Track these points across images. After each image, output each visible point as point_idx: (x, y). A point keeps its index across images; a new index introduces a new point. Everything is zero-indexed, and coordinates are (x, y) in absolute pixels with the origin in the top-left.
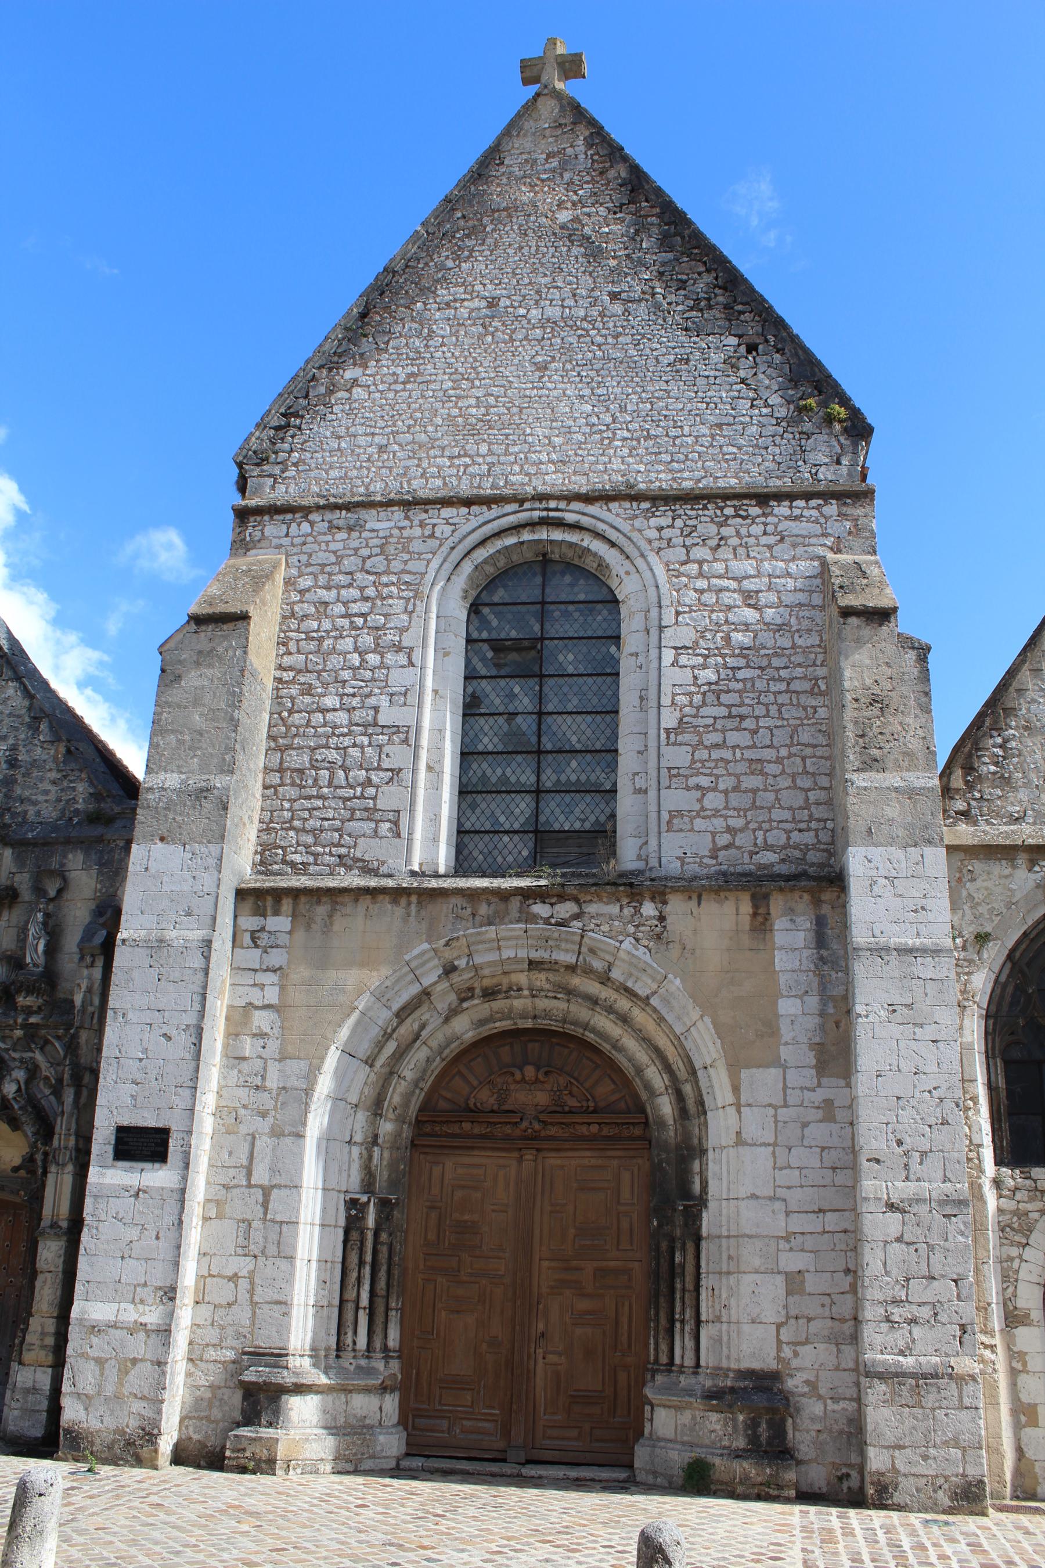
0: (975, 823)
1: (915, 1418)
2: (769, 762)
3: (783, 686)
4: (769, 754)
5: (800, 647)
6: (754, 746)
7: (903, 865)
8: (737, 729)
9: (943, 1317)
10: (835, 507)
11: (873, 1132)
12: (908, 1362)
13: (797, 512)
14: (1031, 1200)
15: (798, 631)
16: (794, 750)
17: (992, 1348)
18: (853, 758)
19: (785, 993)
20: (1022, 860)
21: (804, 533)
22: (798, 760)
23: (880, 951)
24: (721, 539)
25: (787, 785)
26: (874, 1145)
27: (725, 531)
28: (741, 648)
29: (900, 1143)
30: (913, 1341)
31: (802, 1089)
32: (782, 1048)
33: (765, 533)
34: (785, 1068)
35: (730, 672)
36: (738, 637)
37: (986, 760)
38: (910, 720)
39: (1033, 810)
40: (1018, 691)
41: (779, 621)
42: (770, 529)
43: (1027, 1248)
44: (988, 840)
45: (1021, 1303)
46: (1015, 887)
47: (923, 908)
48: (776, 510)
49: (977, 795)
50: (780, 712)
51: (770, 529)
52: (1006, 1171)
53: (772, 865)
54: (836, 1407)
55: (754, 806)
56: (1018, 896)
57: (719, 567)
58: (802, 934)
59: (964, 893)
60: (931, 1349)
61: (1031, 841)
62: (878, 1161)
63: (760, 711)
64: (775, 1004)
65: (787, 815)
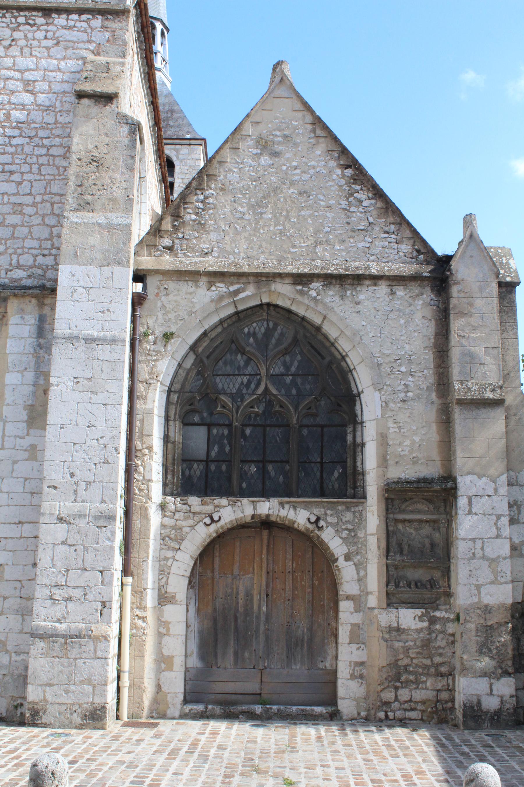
0: (176, 255)
1: (63, 665)
2: (27, 205)
3: (44, 151)
4: (28, 200)
5: (61, 123)
6: (18, 194)
7: (98, 279)
8: (7, 181)
9: (90, 597)
10: (100, 21)
12: (62, 627)
13: (71, 23)
14: (185, 519)
15: (60, 111)
16: (46, 197)
17: (144, 619)
18: (71, 201)
19: (11, 369)
20: (203, 281)
21: (74, 39)
22: (48, 204)
23: (72, 339)
24: (13, 40)
25: (38, 222)
26: (54, 476)
27: (16, 35)
28: (18, 122)
29: (72, 475)
30: (68, 613)
31: (15, 437)
32: (4, 408)
33: (46, 38)
34: (5, 422)
35: (7, 140)
36: (17, 115)
37: (190, 211)
38: (117, 176)
39: (218, 247)
40: (220, 162)
41: (47, 103)
42: (50, 35)
43: (179, 551)
44: (181, 267)
45: (170, 589)
46: (195, 301)
47: (108, 310)
48: (56, 21)
49: (180, 235)
50: (39, 169)
51: (50, 35)
52: (170, 499)
53: (21, 279)
54: (19, 658)
56: (197, 307)
58: (28, 328)
59: (159, 304)
60: (79, 619)
61: (210, 269)
62: (55, 488)
63: (25, 168)
64: (4, 377)
65: (36, 244)
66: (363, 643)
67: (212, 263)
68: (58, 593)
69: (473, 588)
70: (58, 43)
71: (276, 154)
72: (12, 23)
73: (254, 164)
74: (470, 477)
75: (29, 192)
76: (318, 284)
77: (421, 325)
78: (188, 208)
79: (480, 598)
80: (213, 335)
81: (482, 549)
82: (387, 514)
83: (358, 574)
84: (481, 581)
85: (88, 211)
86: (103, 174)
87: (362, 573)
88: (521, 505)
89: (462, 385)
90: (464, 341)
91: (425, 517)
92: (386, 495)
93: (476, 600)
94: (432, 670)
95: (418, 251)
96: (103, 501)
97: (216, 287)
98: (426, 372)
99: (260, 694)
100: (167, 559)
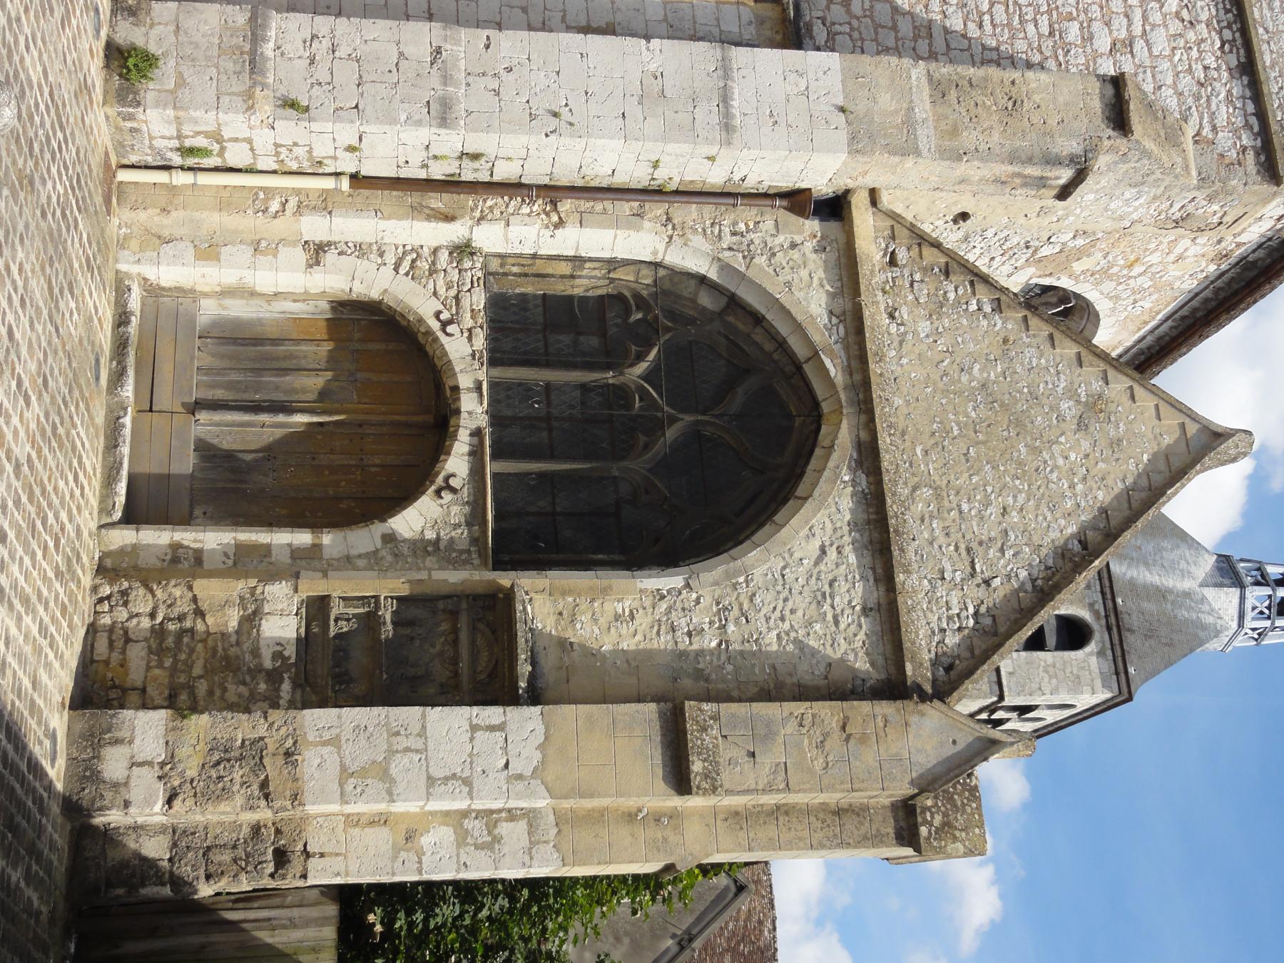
2: (930, 45)
11: (519, 44)
12: (268, 49)
21: (1214, 107)
31: (564, 11)
33: (1206, 68)
36: (1073, 32)
38: (996, 137)
45: (330, 257)
53: (812, 37)
55: (877, 26)
57: (1156, 17)
60: (281, 75)
61: (866, 313)
62: (487, 47)
66: (235, 563)
67: (875, 315)
68: (321, 47)
69: (334, 732)
70: (1202, 85)
71: (1082, 425)
72: (1218, 22)
73: (1060, 390)
74: (541, 729)
75: (953, 46)
76: (864, 483)
77: (814, 662)
78: (965, 287)
79: (315, 745)
80: (758, 336)
81: (407, 750)
82: (468, 596)
83: (359, 556)
84: (347, 749)
85: (931, 96)
86: (995, 117)
87: (361, 563)
88: (492, 849)
89: (711, 718)
90: (791, 727)
91: (464, 665)
92: (501, 596)
93: (311, 737)
94: (182, 679)
95: (949, 669)
96: (469, 113)
97: (837, 325)
98: (730, 668)
99: (151, 410)
100: (381, 255)
